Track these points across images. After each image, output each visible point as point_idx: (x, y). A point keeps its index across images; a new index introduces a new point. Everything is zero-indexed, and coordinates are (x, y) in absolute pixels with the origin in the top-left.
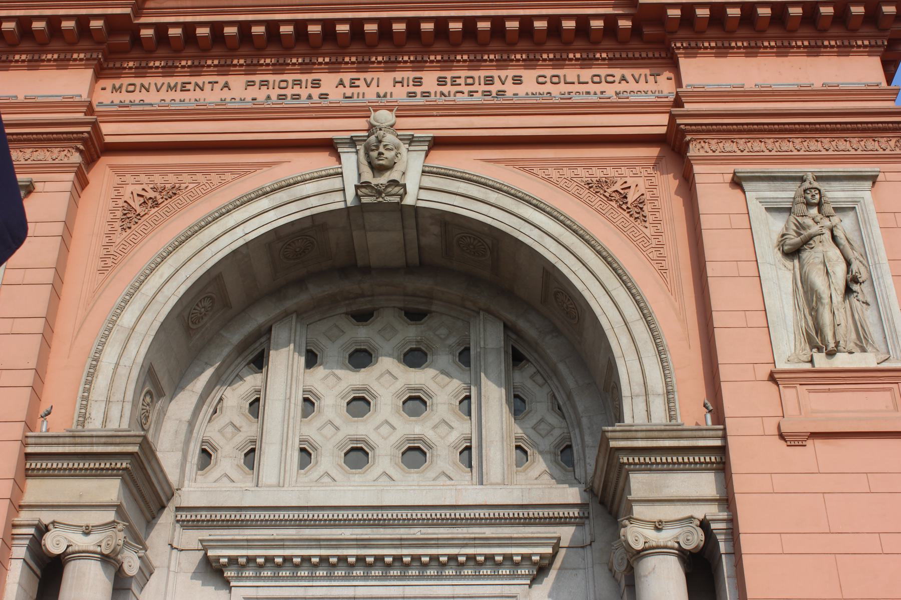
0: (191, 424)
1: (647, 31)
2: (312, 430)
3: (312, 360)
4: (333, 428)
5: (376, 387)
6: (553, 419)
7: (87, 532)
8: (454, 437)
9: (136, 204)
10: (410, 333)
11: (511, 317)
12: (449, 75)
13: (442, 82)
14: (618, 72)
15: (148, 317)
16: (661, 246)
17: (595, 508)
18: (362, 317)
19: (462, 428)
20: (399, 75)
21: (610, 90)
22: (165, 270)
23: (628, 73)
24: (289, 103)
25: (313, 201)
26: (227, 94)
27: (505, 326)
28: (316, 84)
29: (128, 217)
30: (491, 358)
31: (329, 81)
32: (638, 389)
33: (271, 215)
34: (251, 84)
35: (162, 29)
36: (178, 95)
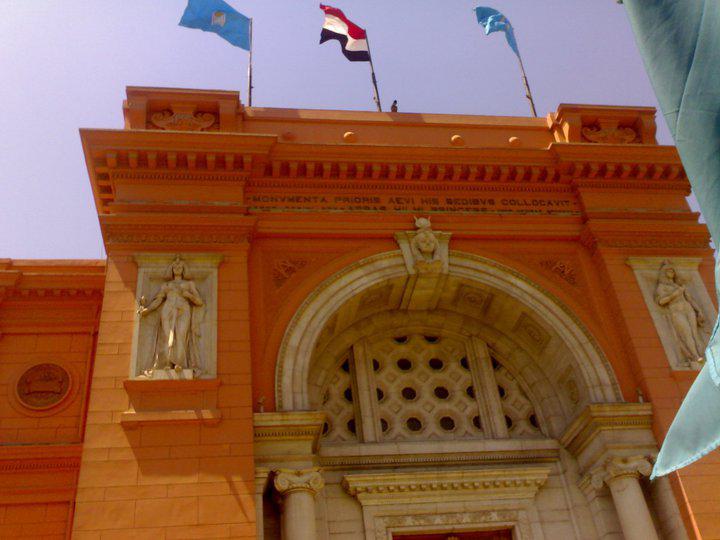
2: (385, 408)
3: (376, 366)
4: (398, 409)
6: (522, 399)
7: (299, 474)
8: (469, 410)
9: (282, 271)
10: (432, 351)
11: (492, 339)
13: (449, 201)
15: (306, 340)
17: (563, 451)
18: (401, 340)
19: (471, 408)
27: (488, 346)
29: (279, 280)
30: (484, 364)
32: (595, 383)
33: (365, 280)
36: (296, 204)
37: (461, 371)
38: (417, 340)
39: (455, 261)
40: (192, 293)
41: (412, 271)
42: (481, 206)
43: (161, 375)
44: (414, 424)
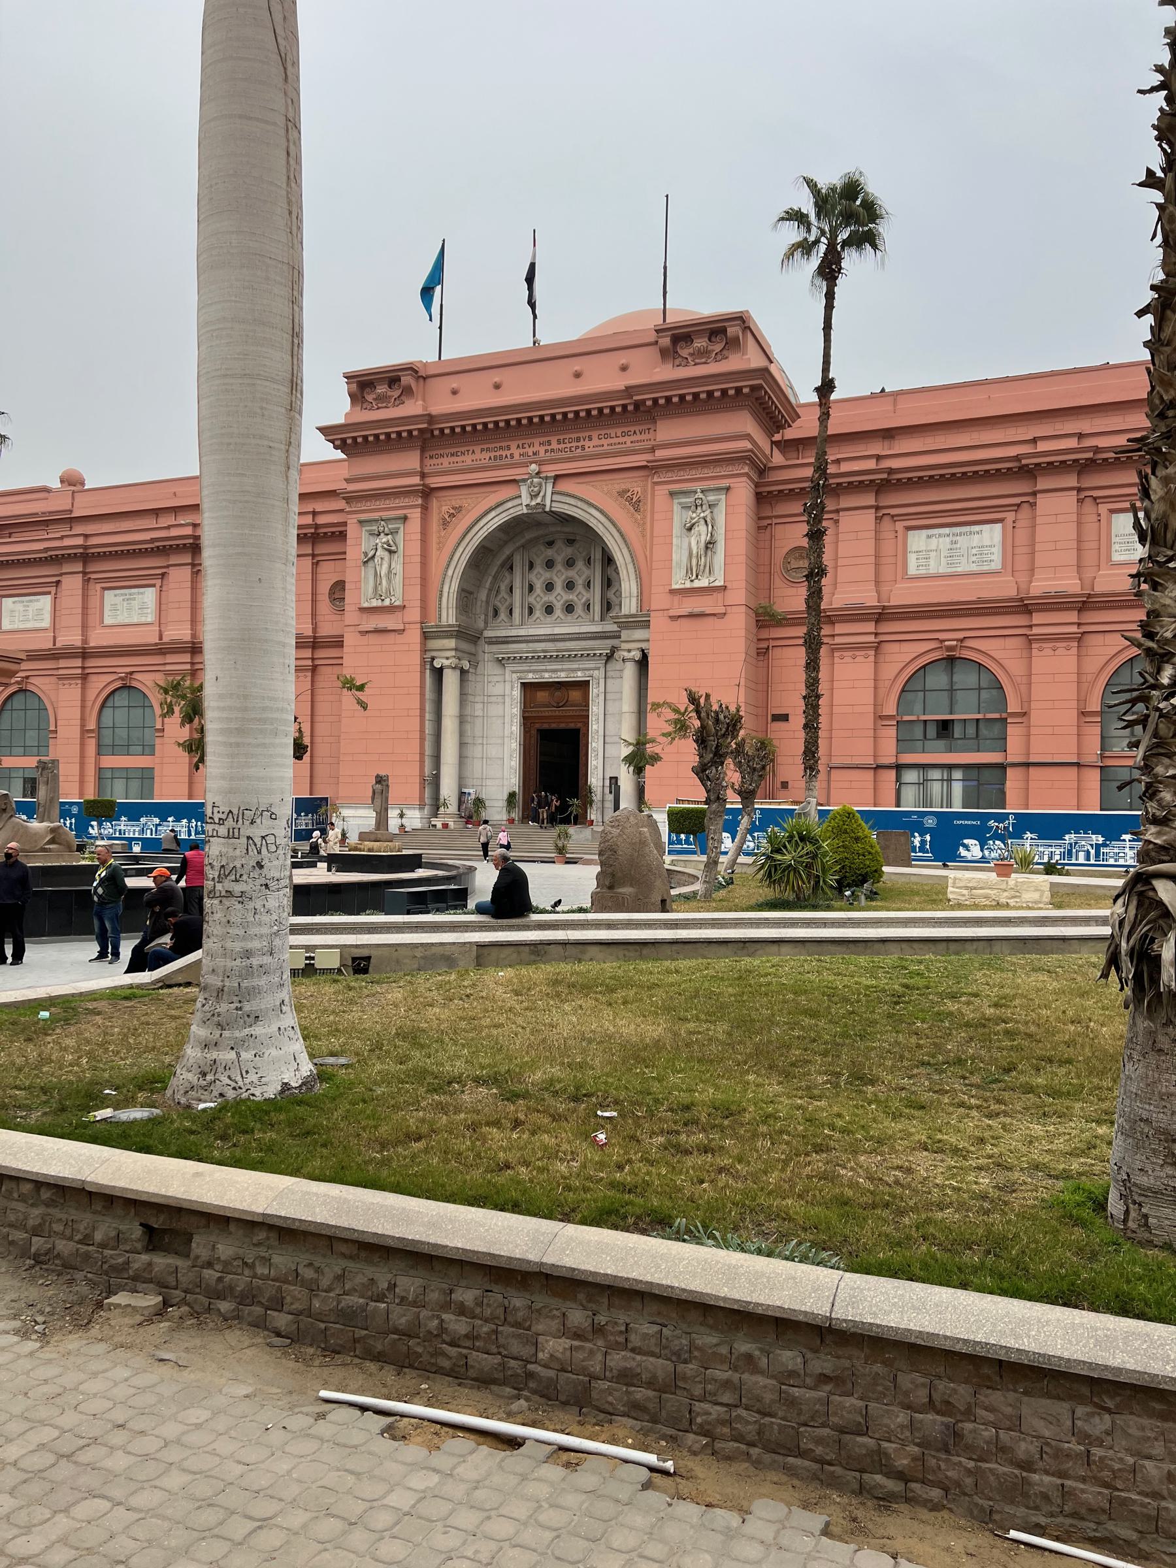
0: (487, 602)
1: (642, 409)
2: (531, 599)
4: (539, 598)
5: (555, 578)
7: (447, 658)
10: (568, 551)
12: (561, 437)
13: (559, 442)
14: (632, 429)
16: (644, 524)
18: (550, 544)
20: (542, 440)
21: (628, 439)
22: (461, 549)
23: (637, 428)
24: (498, 462)
25: (512, 511)
26: (474, 457)
28: (509, 448)
29: (445, 524)
31: (513, 445)
33: (496, 519)
34: (482, 450)
35: (442, 430)
36: (455, 459)
37: (584, 569)
38: (559, 544)
39: (556, 497)
40: (389, 545)
41: (525, 511)
42: (579, 444)
43: (375, 603)
44: (549, 610)
